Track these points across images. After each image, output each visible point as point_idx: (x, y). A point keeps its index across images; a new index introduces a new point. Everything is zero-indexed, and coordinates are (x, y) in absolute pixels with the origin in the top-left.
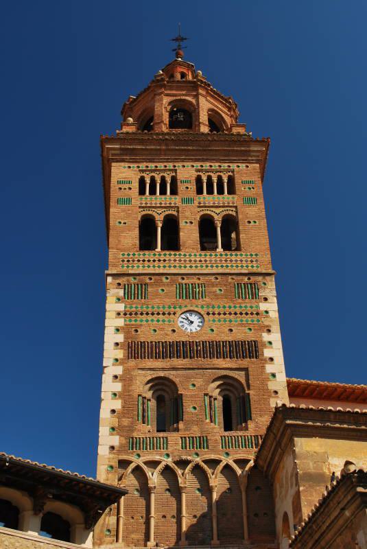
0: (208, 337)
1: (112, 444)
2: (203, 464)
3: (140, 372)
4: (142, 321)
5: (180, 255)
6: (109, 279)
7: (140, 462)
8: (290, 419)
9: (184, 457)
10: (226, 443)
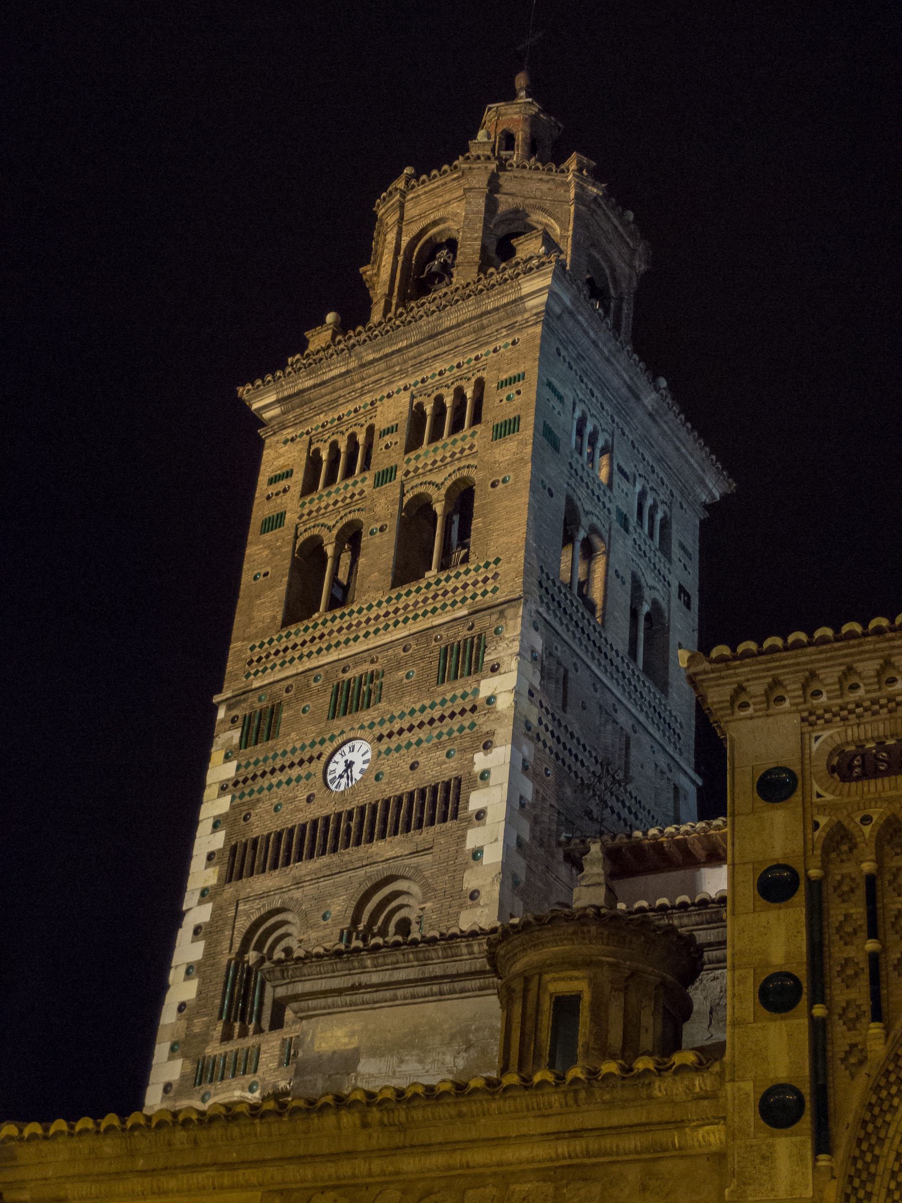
1: (167, 1079)
6: (221, 714)
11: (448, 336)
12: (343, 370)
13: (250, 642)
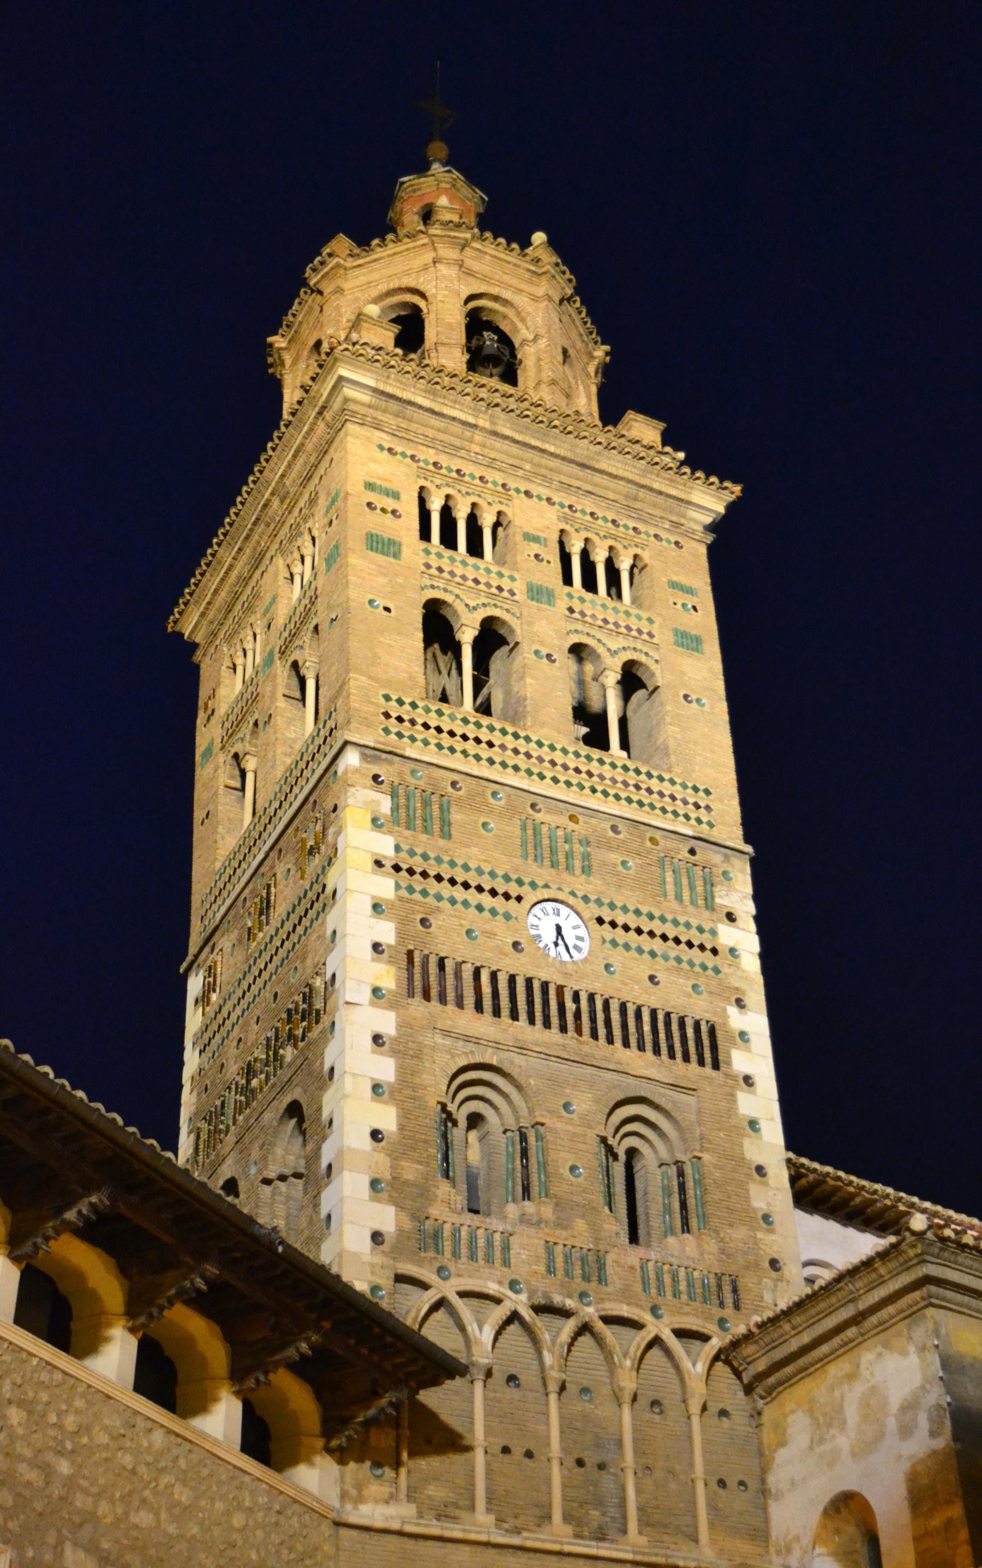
0: (602, 986)
1: (377, 1227)
2: (600, 1326)
3: (439, 1039)
4: (439, 897)
5: (528, 739)
6: (351, 758)
7: (449, 1288)
9: (558, 1299)
11: (598, 478)
12: (471, 420)
13: (384, 687)
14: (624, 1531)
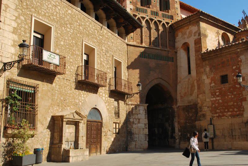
2: (157, 21)
8: (201, 16)
9: (152, 18)
10: (164, 16)
14: (159, 46)
